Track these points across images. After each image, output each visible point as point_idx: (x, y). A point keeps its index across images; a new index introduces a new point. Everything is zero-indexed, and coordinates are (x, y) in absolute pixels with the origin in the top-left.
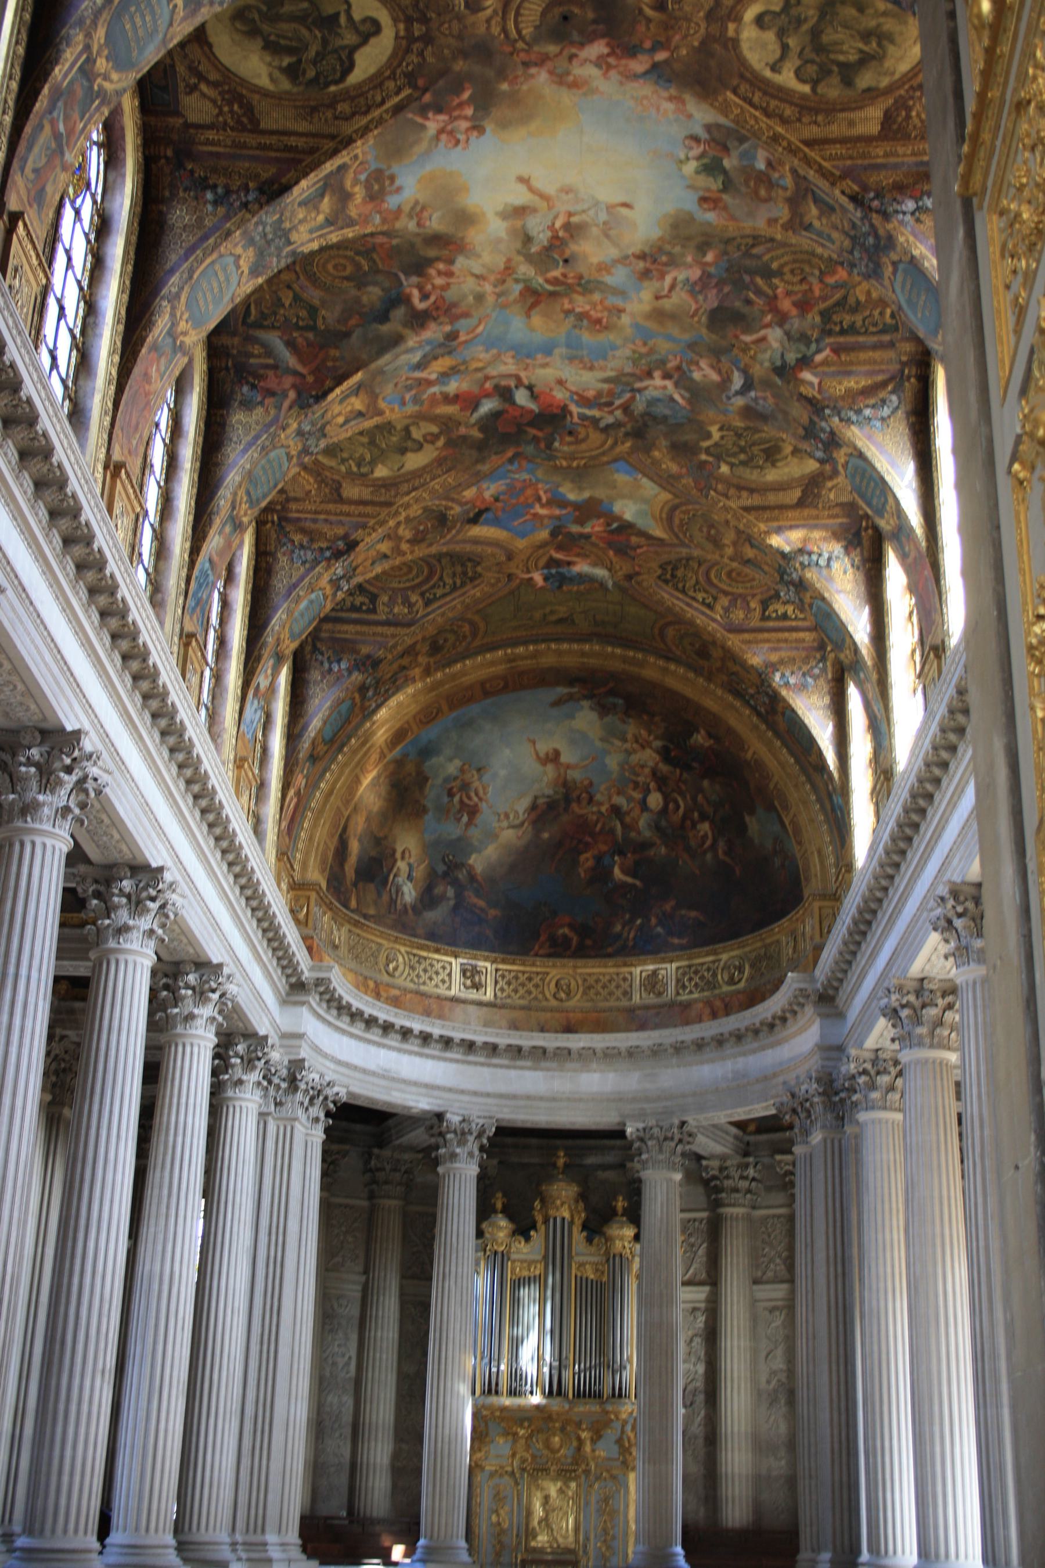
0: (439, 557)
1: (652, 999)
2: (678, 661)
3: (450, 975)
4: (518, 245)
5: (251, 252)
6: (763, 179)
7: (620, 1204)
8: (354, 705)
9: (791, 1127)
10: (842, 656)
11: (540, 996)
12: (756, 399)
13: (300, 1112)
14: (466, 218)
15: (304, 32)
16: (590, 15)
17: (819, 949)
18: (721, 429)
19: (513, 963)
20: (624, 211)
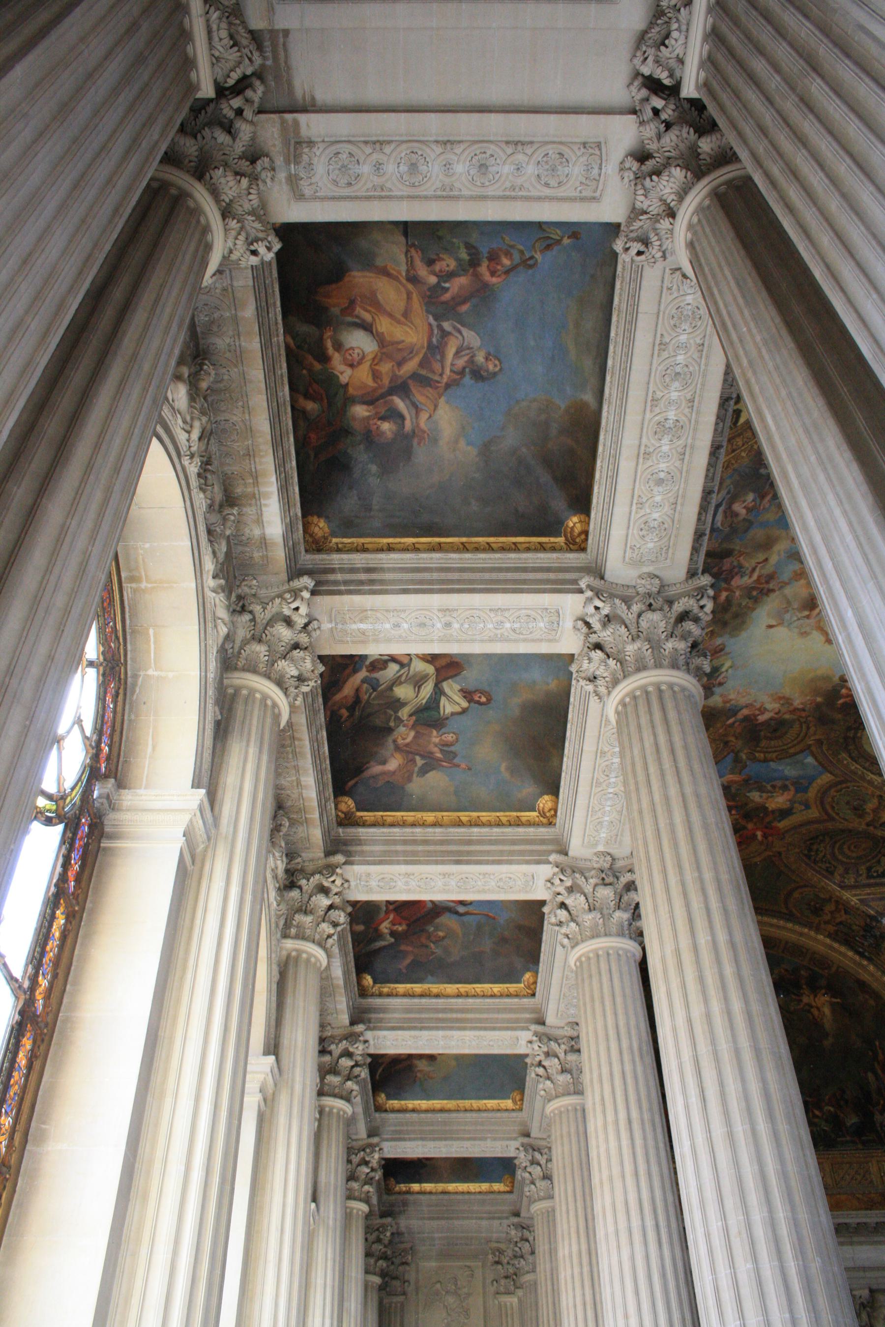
16: (762, 733)
20: (773, 623)
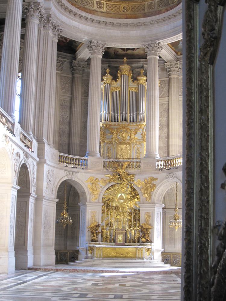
1: (151, 10)
3: (93, 4)
11: (119, 11)
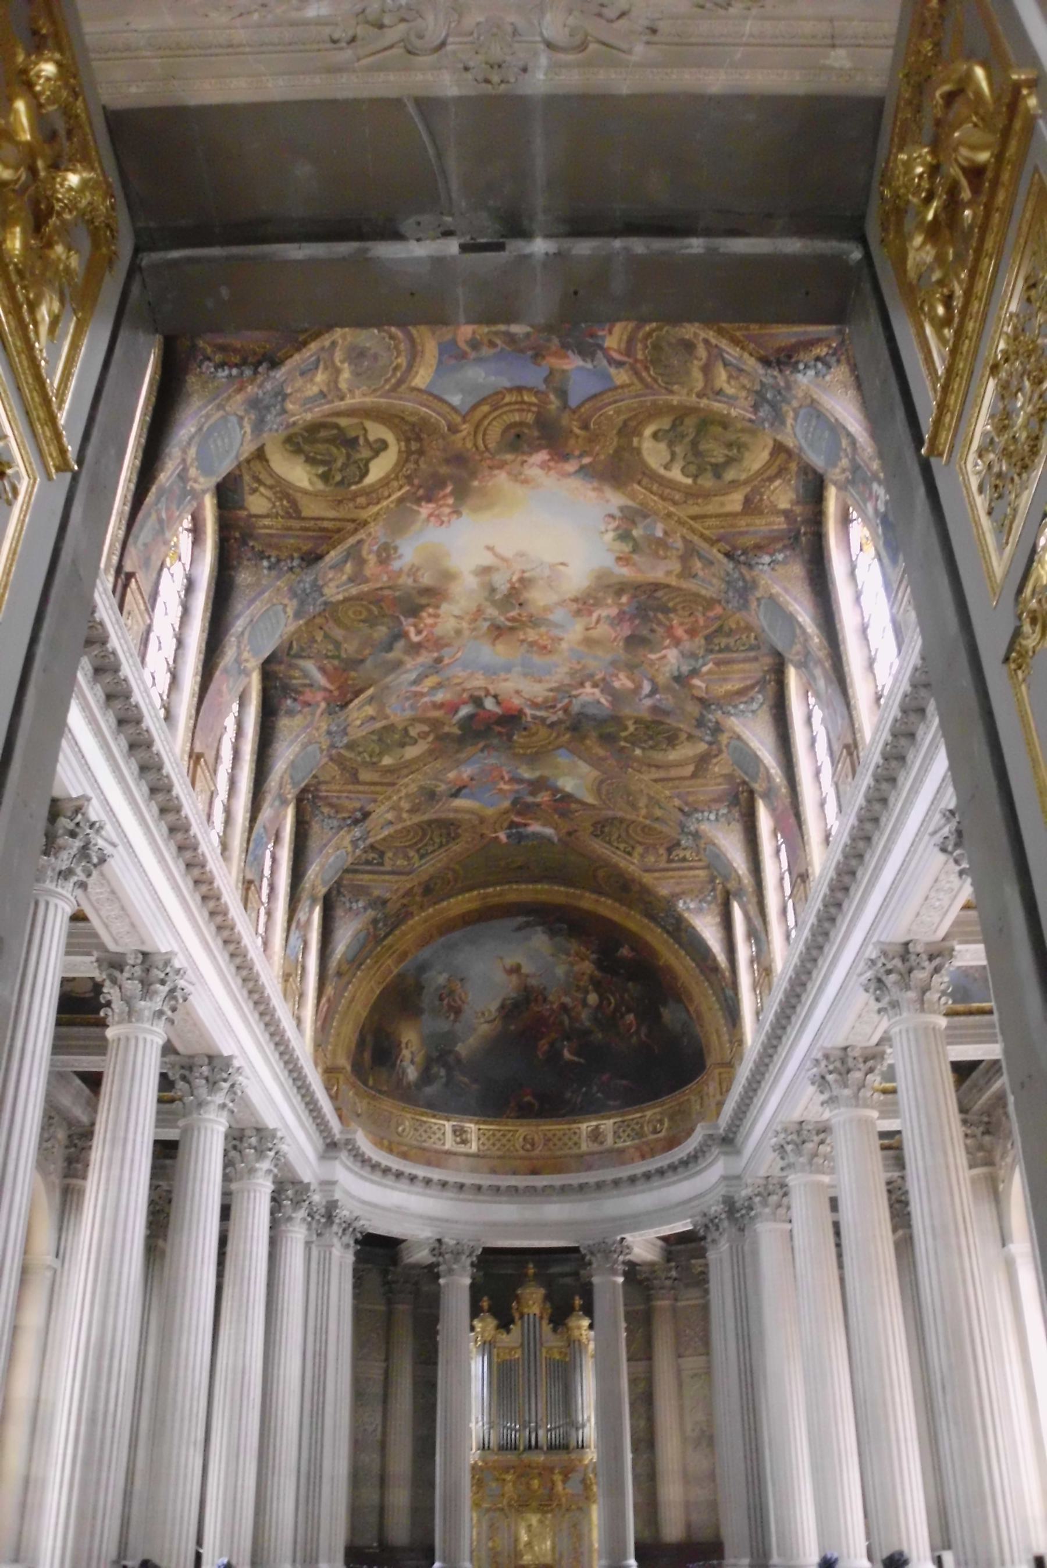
0: (430, 823)
1: (595, 1147)
2: (607, 895)
4: (486, 594)
5: (295, 602)
6: (661, 543)
7: (578, 1302)
8: (368, 934)
9: (704, 1238)
10: (729, 886)
12: (660, 700)
13: (335, 1240)
14: (448, 576)
15: (334, 450)
17: (720, 1104)
18: (635, 723)
19: (491, 1124)
20: (561, 568)
